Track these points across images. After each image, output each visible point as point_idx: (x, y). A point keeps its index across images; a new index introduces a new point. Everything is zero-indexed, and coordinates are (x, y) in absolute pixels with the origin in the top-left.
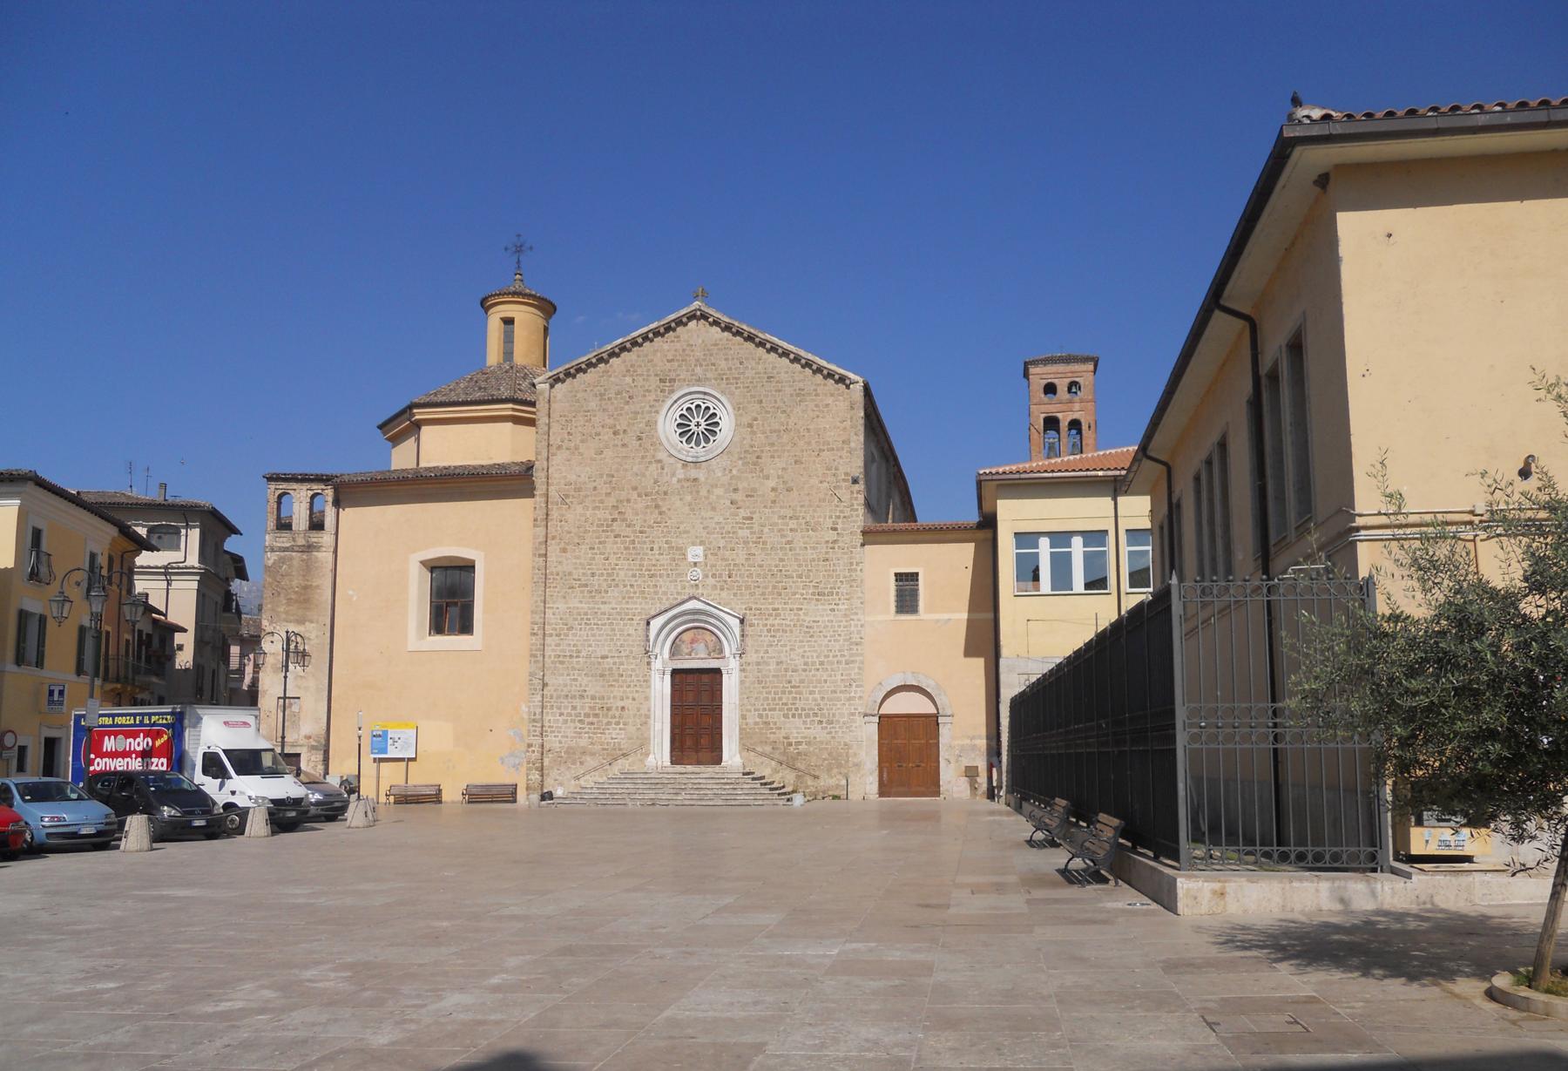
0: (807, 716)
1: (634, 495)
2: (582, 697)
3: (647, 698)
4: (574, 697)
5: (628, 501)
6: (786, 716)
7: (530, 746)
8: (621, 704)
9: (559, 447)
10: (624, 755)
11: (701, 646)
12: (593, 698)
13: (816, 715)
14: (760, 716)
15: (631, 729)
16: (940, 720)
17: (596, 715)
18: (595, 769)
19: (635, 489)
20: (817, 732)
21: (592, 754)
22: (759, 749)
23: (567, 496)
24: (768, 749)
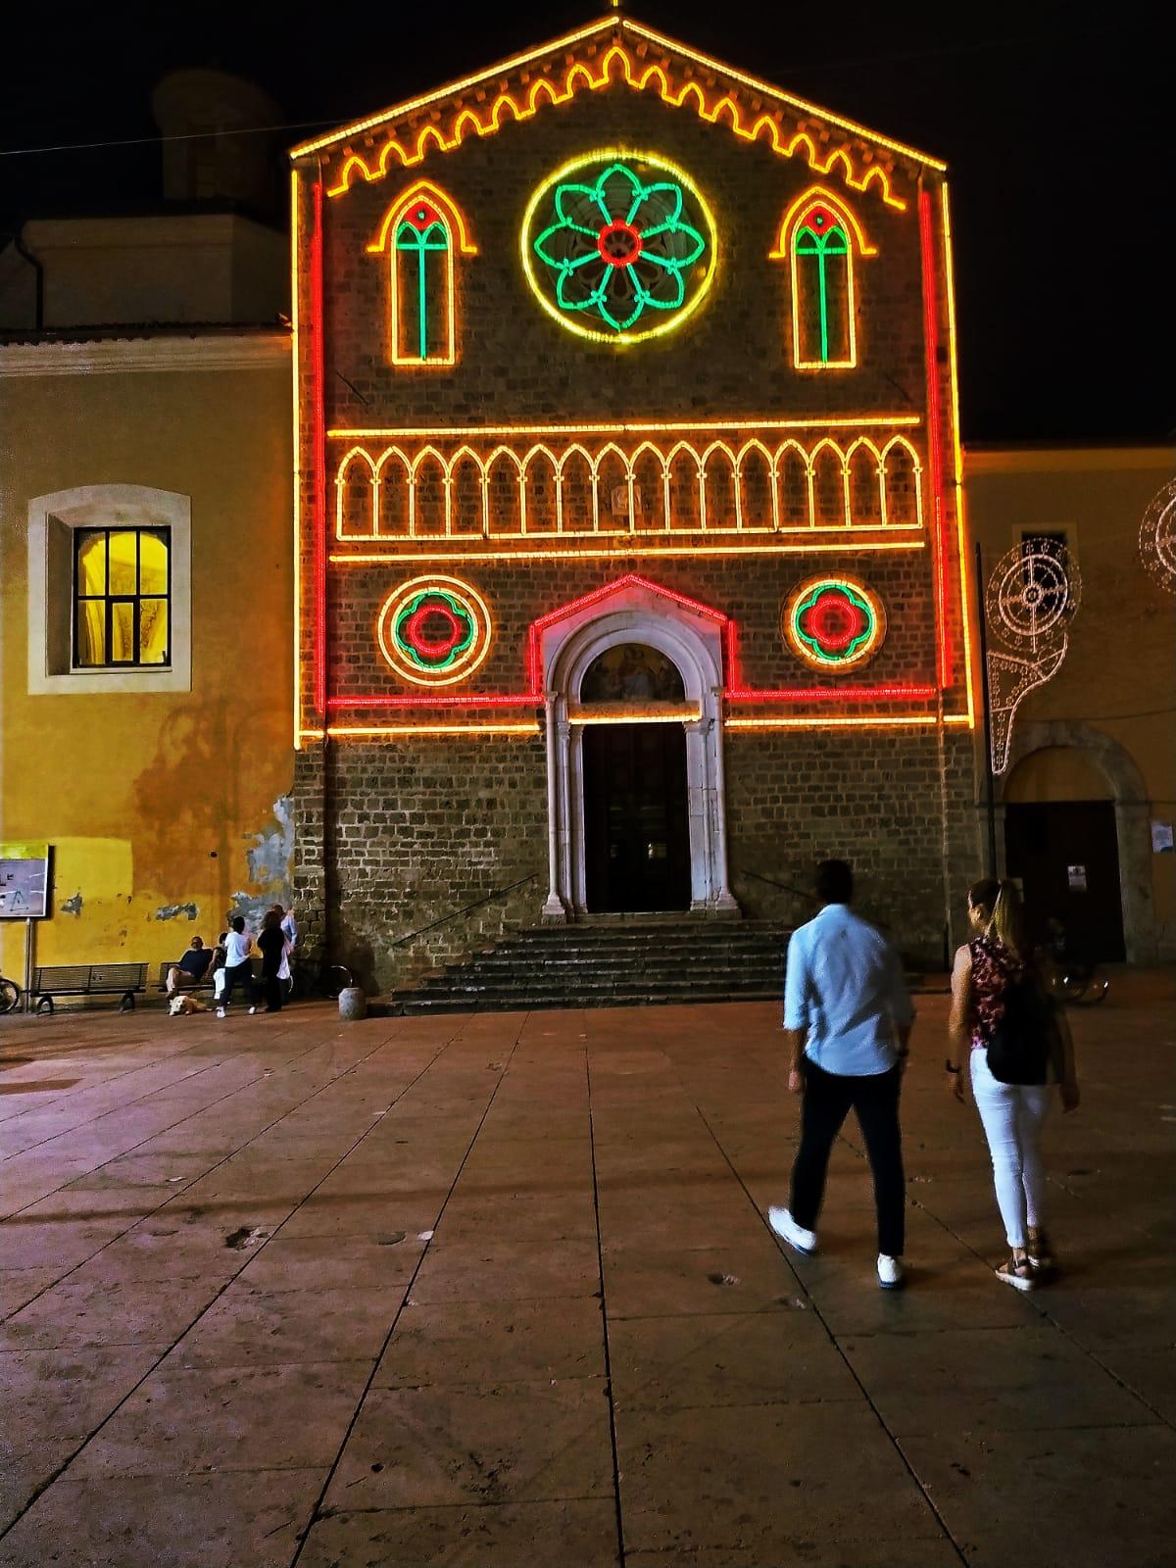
0: (859, 810)
1: (500, 385)
2: (405, 782)
3: (541, 783)
4: (389, 783)
5: (489, 396)
6: (818, 812)
7: (300, 882)
8: (484, 794)
9: (344, 287)
10: (497, 895)
11: (642, 681)
12: (429, 783)
13: (875, 809)
14: (767, 813)
15: (507, 842)
16: (1119, 811)
17: (436, 819)
18: (437, 926)
19: (501, 372)
20: (875, 840)
21: (429, 896)
22: (769, 876)
23: (364, 385)
24: (784, 876)
